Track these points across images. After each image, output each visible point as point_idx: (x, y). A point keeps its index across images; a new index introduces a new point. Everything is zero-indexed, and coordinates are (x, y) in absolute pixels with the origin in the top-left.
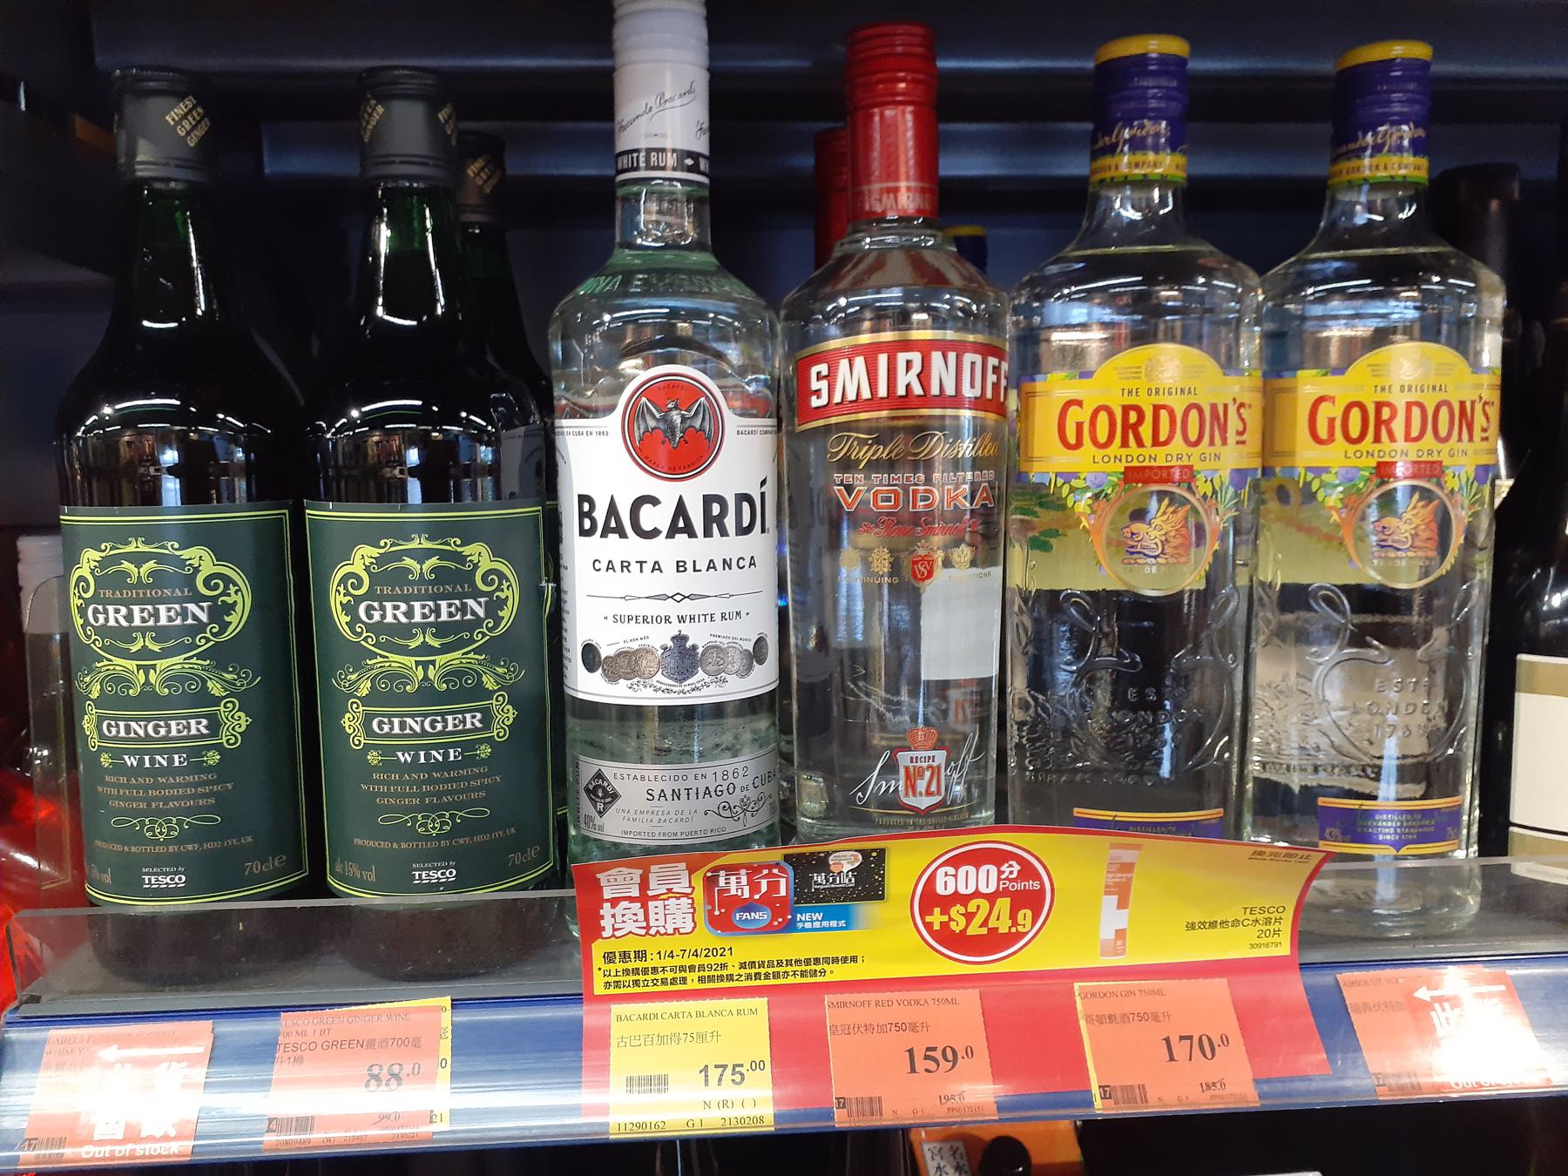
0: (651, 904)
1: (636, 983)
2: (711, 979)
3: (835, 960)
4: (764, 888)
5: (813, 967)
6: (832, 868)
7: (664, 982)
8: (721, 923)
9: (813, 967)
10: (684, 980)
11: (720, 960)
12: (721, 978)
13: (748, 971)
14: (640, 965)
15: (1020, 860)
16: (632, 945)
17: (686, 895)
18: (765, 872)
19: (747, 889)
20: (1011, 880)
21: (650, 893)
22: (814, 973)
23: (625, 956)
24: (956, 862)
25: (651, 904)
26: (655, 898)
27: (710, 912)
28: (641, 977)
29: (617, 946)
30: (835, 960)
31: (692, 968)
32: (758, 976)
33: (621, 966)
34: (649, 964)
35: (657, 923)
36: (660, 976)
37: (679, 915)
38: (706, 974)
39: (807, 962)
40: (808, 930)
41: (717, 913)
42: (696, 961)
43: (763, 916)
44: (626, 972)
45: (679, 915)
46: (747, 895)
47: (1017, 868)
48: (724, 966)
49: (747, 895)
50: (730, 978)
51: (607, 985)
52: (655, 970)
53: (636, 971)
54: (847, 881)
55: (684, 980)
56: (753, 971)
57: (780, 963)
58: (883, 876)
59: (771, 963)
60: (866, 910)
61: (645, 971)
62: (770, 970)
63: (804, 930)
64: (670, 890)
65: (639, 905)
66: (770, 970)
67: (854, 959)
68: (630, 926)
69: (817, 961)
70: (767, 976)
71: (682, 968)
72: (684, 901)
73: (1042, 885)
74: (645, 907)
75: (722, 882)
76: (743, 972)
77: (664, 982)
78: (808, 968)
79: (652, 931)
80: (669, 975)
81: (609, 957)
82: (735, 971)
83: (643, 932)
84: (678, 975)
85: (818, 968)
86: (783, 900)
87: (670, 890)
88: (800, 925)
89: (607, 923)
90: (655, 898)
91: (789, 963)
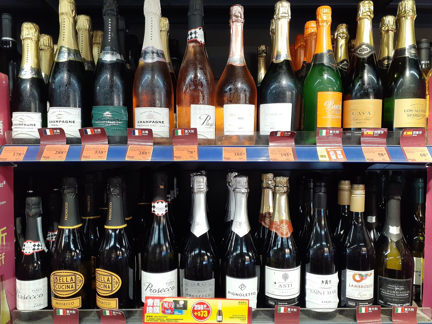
0: (154, 307)
1: (151, 321)
2: (162, 321)
3: (180, 319)
4: (170, 306)
5: (176, 320)
6: (180, 304)
7: (155, 321)
8: (164, 312)
9: (176, 320)
10: (158, 321)
11: (163, 318)
12: (163, 321)
13: (167, 320)
14: (152, 318)
15: (207, 305)
16: (151, 315)
17: (159, 306)
18: (170, 303)
19: (167, 306)
20: (205, 308)
21: (154, 305)
22: (177, 321)
23: (150, 316)
24: (197, 304)
25: (154, 307)
26: (155, 306)
27: (162, 310)
28: (152, 320)
29: (148, 315)
30: (180, 319)
31: (159, 319)
32: (168, 321)
33: (149, 318)
34: (153, 318)
35: (155, 311)
36: (154, 320)
37: (158, 310)
38: (161, 320)
39: (176, 319)
40: (176, 314)
41: (163, 310)
42: (160, 318)
43: (170, 311)
44: (150, 319)
45: (158, 310)
46: (167, 307)
47: (206, 306)
48: (164, 319)
49: (167, 307)
50: (164, 321)
51: (147, 321)
52: (154, 319)
53: (151, 319)
54: (182, 306)
55: (158, 321)
56: (168, 320)
57: (172, 319)
58: (187, 306)
59: (170, 319)
60: (184, 311)
61: (152, 319)
62: (170, 320)
63: (175, 314)
64: (157, 305)
65: (152, 307)
66: (170, 320)
67: (183, 319)
68: (151, 312)
69: (177, 319)
70: (170, 321)
71: (158, 319)
72: (159, 307)
73: (210, 309)
74: (153, 308)
75: (164, 304)
76: (166, 320)
77: (155, 321)
78: (176, 320)
79: (154, 313)
80: (156, 320)
81: (147, 316)
82: (165, 320)
83: (152, 313)
84: (157, 320)
85: (177, 320)
86: (172, 309)
87: (157, 305)
88: (175, 313)
89: (147, 310)
90: (155, 306)
91: (173, 319)
